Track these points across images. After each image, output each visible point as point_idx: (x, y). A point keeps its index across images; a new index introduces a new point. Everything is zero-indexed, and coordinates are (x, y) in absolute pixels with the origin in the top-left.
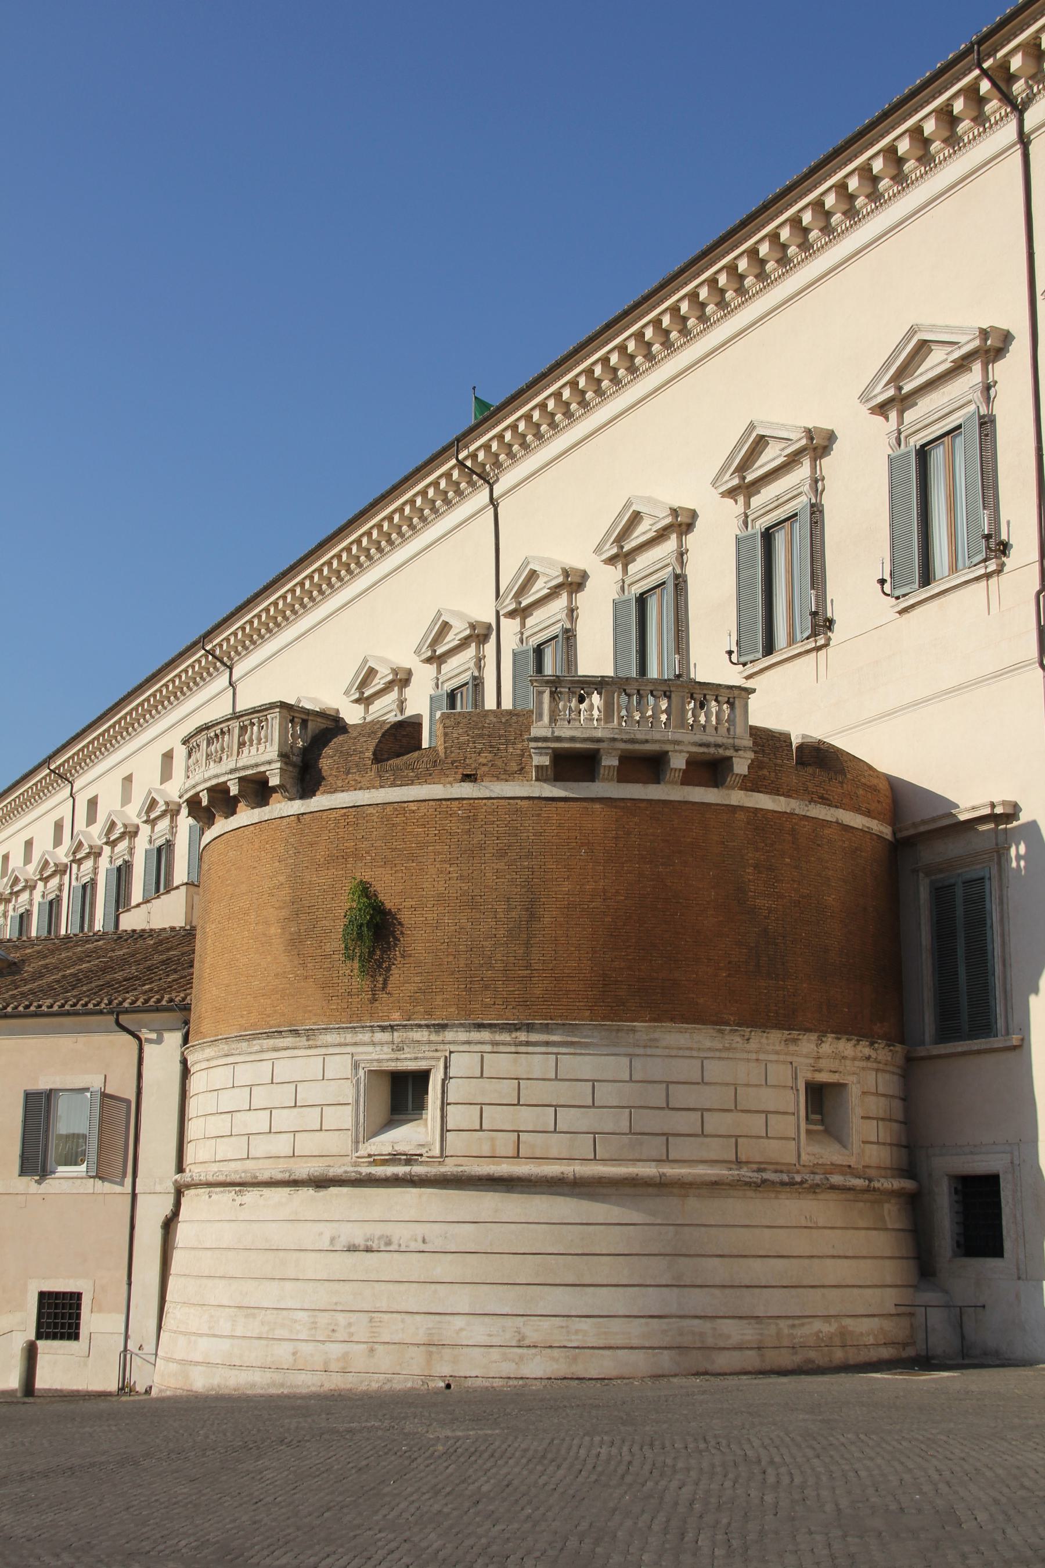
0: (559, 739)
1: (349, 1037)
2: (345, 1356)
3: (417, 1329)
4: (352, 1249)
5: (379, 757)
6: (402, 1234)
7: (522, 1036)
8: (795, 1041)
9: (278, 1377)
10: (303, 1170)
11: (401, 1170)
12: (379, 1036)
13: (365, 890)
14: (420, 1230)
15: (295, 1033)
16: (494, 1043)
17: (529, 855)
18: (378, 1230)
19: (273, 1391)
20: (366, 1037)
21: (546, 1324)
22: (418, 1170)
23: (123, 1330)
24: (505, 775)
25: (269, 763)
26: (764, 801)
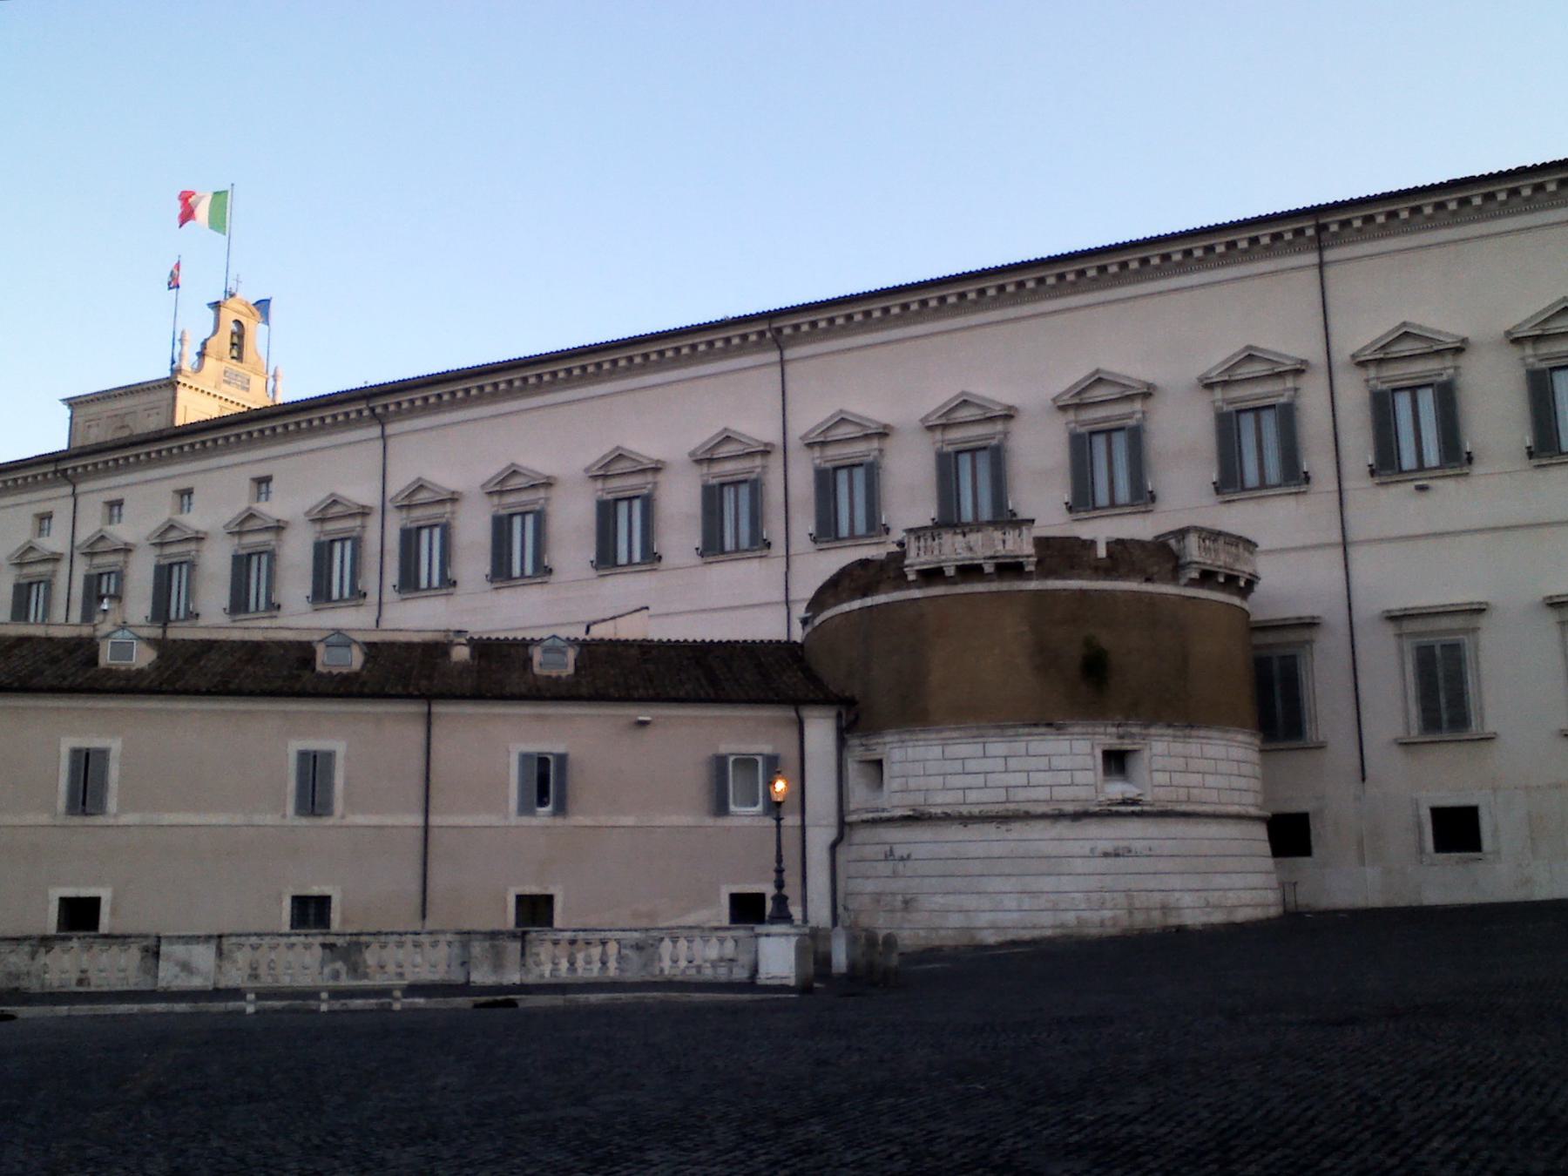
0: (1204, 564)
3: (1157, 898)
4: (1106, 855)
6: (1138, 846)
11: (1136, 808)
25: (1028, 556)
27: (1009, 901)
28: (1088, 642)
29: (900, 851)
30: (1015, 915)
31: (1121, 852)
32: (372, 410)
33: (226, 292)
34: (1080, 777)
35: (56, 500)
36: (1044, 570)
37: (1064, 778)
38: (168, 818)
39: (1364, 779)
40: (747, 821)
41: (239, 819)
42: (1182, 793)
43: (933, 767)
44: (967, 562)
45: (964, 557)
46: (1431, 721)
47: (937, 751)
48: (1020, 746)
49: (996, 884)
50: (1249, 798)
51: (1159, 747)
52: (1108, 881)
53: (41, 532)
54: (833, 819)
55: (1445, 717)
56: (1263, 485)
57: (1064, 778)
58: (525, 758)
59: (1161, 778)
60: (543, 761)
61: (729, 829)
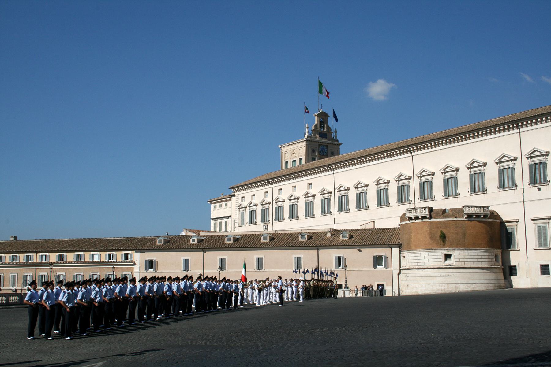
1: (441, 250)
2: (444, 289)
3: (454, 285)
4: (444, 276)
5: (442, 215)
6: (451, 274)
7: (465, 250)
8: (494, 250)
9: (434, 292)
10: (436, 267)
11: (450, 267)
12: (445, 250)
13: (442, 232)
14: (453, 274)
15: (433, 249)
16: (461, 251)
17: (464, 228)
18: (447, 274)
19: (434, 293)
20: (444, 250)
21: (470, 284)
22: (453, 266)
23: (392, 288)
24: (460, 217)
26: (490, 220)
27: (424, 286)
28: (442, 232)
29: (407, 276)
30: (425, 288)
31: (447, 276)
32: (330, 168)
33: (319, 109)
34: (439, 260)
35: (268, 188)
36: (431, 217)
37: (436, 260)
38: (273, 270)
39: (527, 258)
40: (380, 269)
41: (285, 270)
42: (463, 263)
43: (412, 258)
44: (416, 216)
45: (415, 215)
46: (540, 245)
47: (413, 255)
48: (427, 254)
49: (422, 282)
50: (486, 263)
51: (457, 253)
52: (444, 282)
53: (265, 196)
54: (399, 269)
55: (543, 243)
56: (509, 187)
57: (436, 260)
58: (336, 257)
59: (457, 260)
60: (339, 258)
61: (377, 271)
